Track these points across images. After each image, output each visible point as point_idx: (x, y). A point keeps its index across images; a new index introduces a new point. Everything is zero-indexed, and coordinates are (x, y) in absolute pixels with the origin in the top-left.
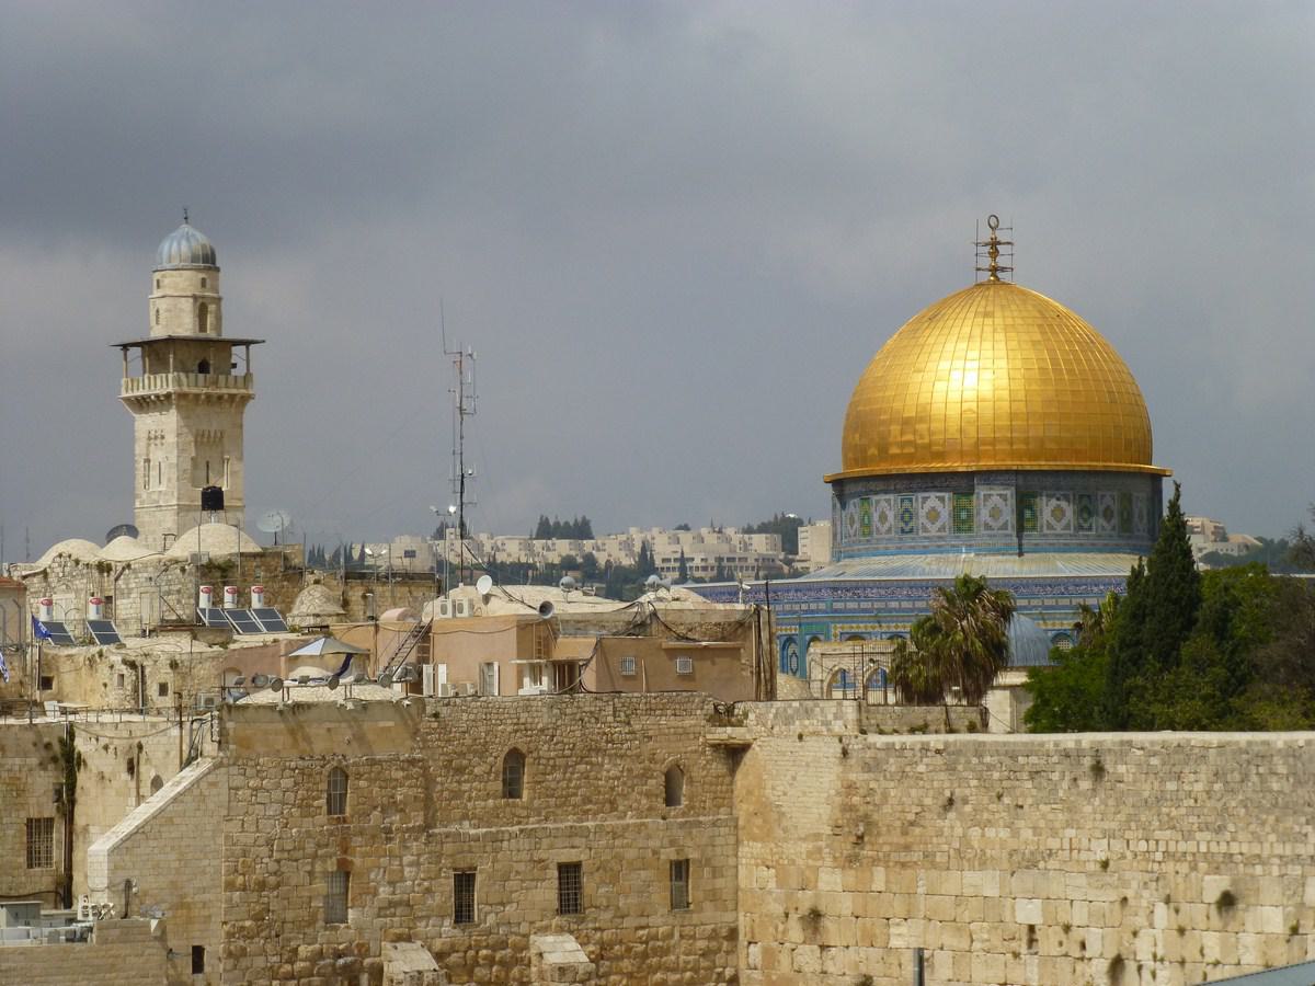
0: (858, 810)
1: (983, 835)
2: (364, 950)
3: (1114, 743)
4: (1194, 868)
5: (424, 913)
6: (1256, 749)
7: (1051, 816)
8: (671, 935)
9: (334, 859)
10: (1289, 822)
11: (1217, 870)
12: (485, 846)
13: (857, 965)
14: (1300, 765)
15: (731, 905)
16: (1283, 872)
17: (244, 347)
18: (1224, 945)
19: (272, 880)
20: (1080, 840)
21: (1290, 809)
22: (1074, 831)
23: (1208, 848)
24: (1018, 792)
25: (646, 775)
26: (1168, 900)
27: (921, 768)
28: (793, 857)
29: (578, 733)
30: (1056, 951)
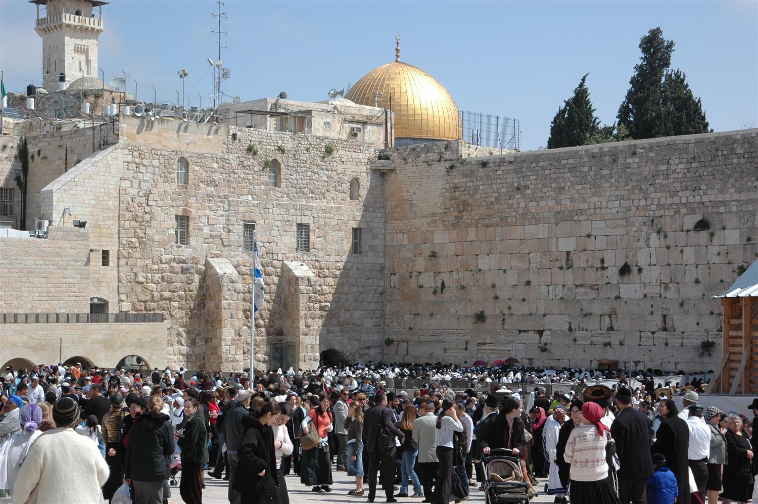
2: (195, 261)
3: (624, 146)
4: (678, 212)
7: (583, 191)
11: (693, 211)
12: (260, 210)
13: (458, 280)
16: (740, 209)
20: (601, 203)
22: (597, 198)
23: (687, 200)
24: (561, 180)
25: (340, 182)
26: (658, 232)
29: (307, 155)
30: (584, 265)
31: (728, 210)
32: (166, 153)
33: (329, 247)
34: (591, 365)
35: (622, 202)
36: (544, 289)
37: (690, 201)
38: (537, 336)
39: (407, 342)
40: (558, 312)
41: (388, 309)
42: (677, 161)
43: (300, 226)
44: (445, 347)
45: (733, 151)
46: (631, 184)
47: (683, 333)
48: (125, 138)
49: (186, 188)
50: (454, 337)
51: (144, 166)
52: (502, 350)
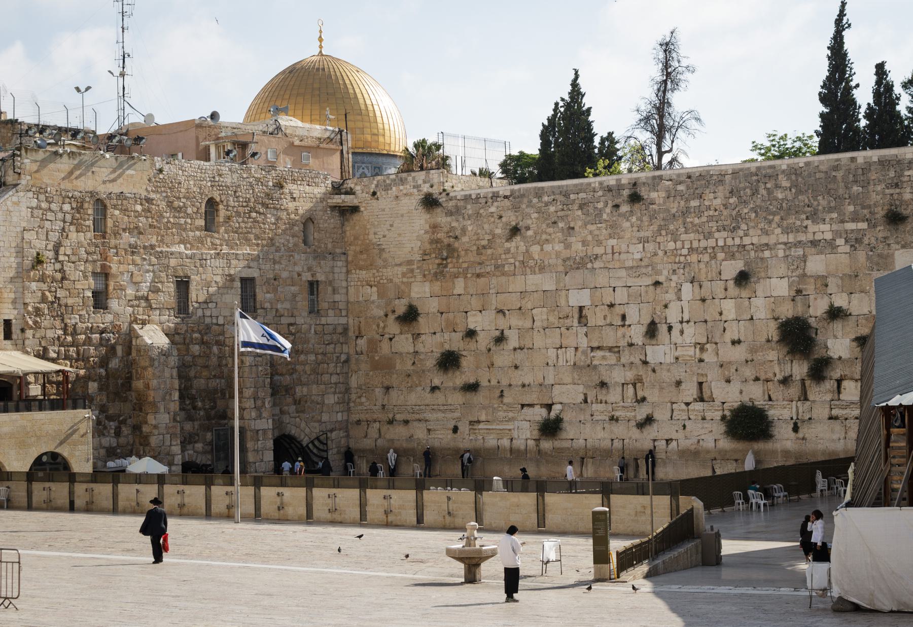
0: (442, 242)
1: (542, 250)
3: (647, 178)
5: (158, 306)
7: (597, 232)
10: (791, 220)
11: (732, 256)
13: (442, 344)
14: (800, 179)
15: (344, 313)
16: (787, 253)
18: (738, 308)
19: (59, 276)
21: (789, 209)
22: (615, 240)
23: (725, 242)
27: (493, 209)
28: (391, 277)
29: (251, 192)
31: (774, 255)
33: (279, 306)
34: (612, 444)
35: (646, 245)
36: (552, 353)
37: (728, 244)
38: (544, 412)
39: (379, 421)
40: (569, 380)
41: (354, 382)
44: (429, 427)
45: (777, 186)
47: (723, 403)
48: (28, 178)
50: (440, 415)
52: (500, 430)
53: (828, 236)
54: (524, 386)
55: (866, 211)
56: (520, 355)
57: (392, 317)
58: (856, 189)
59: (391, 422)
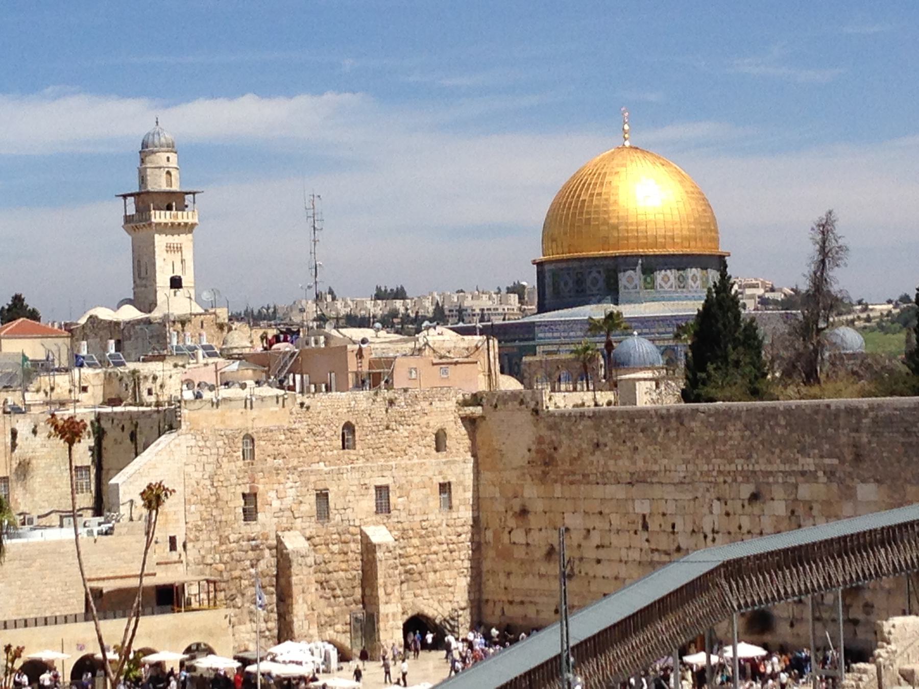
4: (735, 480)
5: (300, 515)
6: (767, 411)
7: (654, 452)
8: (440, 525)
9: (248, 485)
10: (787, 453)
13: (547, 538)
17: (191, 196)
19: (213, 499)
24: (635, 439)
25: (424, 435)
26: (719, 499)
27: (581, 427)
30: (657, 528)
32: (230, 432)
33: (413, 507)
36: (623, 552)
42: (732, 428)
43: (378, 488)
45: (778, 424)
46: (696, 447)
48: (188, 423)
49: (252, 464)
50: (545, 599)
51: (208, 448)
53: (812, 468)
54: (603, 577)
55: (837, 450)
56: (602, 554)
57: (510, 513)
58: (830, 431)
59: (511, 603)
